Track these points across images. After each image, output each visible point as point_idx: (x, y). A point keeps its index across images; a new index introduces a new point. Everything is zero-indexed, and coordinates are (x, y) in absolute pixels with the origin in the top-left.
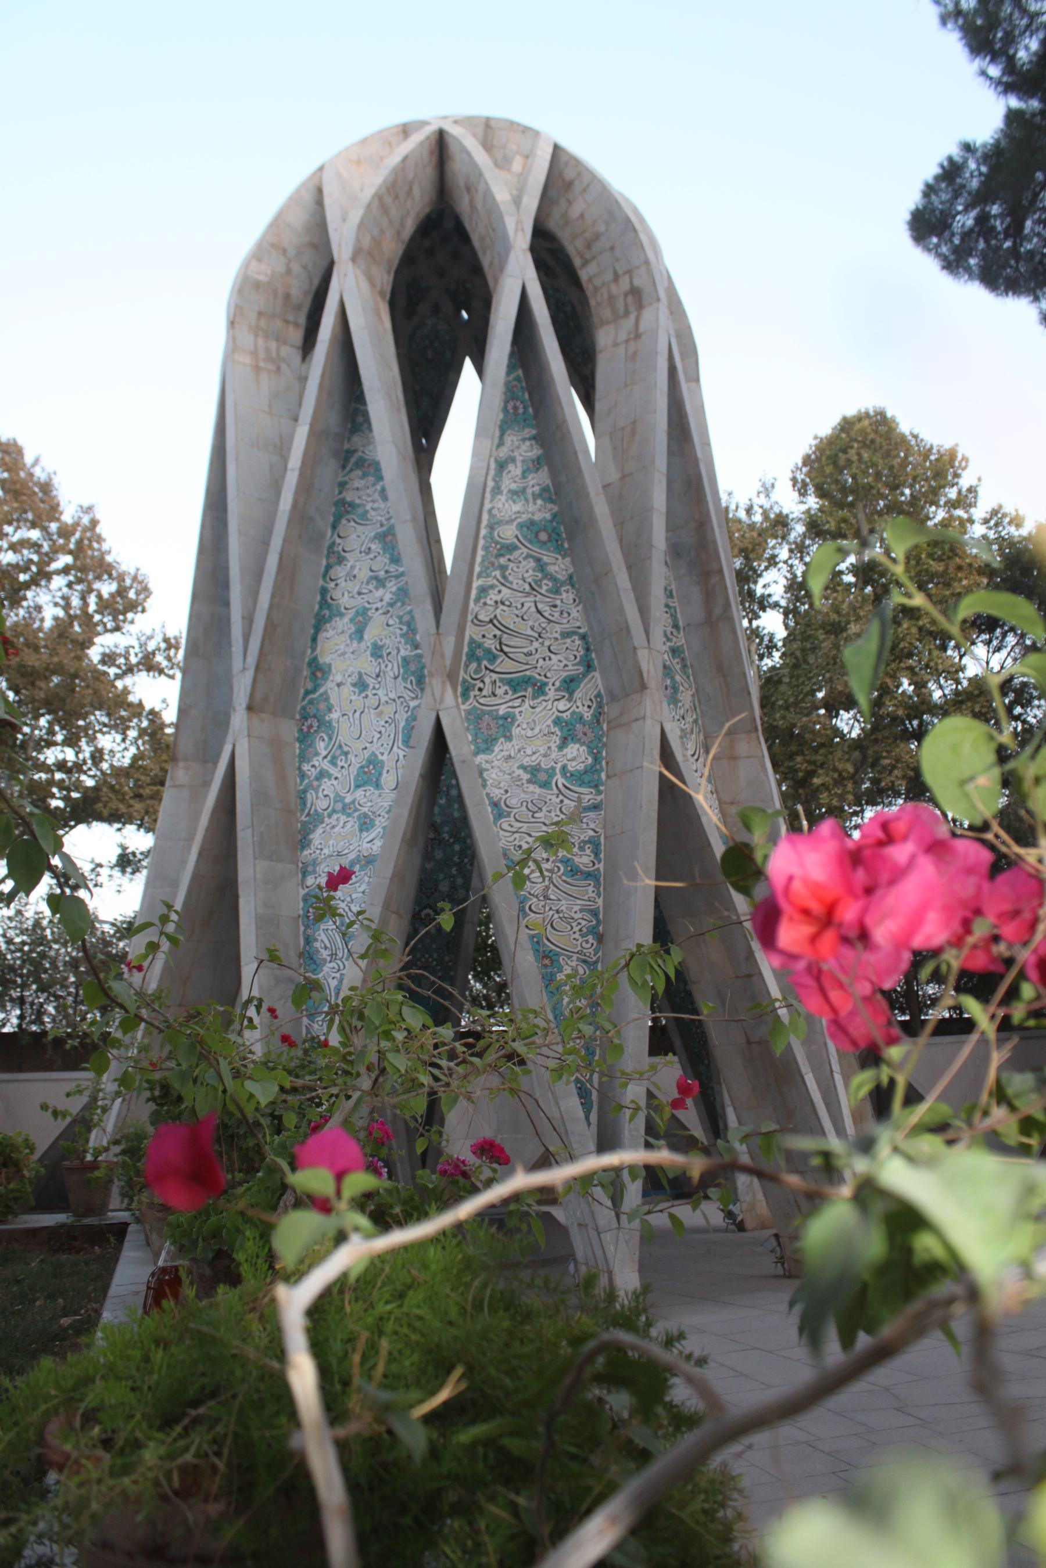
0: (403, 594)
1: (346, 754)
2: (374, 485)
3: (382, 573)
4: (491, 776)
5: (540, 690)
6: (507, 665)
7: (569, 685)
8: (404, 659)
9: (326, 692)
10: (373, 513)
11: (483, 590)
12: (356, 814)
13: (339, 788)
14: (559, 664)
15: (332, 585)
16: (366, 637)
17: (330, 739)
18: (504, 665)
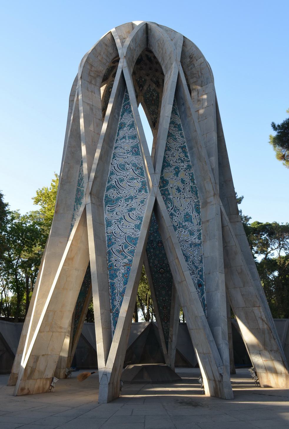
0: (189, 167)
1: (179, 210)
2: (178, 131)
3: (182, 158)
8: (191, 187)
9: (167, 189)
10: (179, 140)
12: (187, 229)
13: (179, 220)
15: (167, 156)
16: (179, 176)
17: (172, 204)
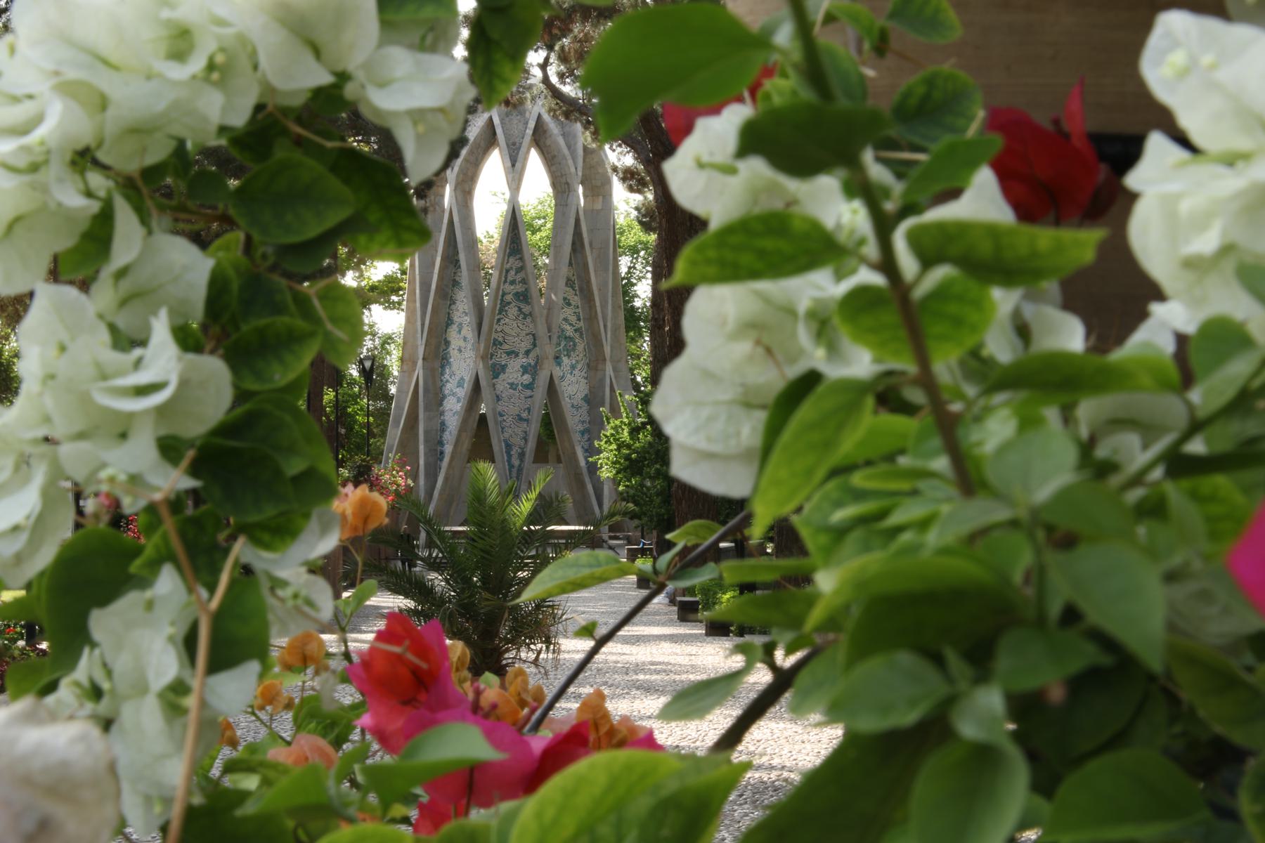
4: (498, 386)
5: (517, 355)
6: (506, 347)
7: (527, 353)
11: (499, 320)
14: (525, 345)
18: (506, 347)
